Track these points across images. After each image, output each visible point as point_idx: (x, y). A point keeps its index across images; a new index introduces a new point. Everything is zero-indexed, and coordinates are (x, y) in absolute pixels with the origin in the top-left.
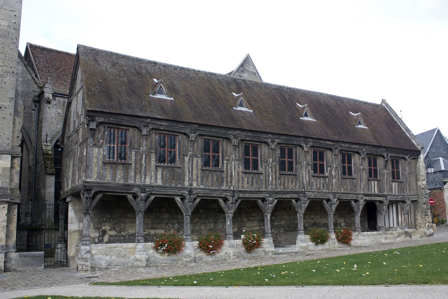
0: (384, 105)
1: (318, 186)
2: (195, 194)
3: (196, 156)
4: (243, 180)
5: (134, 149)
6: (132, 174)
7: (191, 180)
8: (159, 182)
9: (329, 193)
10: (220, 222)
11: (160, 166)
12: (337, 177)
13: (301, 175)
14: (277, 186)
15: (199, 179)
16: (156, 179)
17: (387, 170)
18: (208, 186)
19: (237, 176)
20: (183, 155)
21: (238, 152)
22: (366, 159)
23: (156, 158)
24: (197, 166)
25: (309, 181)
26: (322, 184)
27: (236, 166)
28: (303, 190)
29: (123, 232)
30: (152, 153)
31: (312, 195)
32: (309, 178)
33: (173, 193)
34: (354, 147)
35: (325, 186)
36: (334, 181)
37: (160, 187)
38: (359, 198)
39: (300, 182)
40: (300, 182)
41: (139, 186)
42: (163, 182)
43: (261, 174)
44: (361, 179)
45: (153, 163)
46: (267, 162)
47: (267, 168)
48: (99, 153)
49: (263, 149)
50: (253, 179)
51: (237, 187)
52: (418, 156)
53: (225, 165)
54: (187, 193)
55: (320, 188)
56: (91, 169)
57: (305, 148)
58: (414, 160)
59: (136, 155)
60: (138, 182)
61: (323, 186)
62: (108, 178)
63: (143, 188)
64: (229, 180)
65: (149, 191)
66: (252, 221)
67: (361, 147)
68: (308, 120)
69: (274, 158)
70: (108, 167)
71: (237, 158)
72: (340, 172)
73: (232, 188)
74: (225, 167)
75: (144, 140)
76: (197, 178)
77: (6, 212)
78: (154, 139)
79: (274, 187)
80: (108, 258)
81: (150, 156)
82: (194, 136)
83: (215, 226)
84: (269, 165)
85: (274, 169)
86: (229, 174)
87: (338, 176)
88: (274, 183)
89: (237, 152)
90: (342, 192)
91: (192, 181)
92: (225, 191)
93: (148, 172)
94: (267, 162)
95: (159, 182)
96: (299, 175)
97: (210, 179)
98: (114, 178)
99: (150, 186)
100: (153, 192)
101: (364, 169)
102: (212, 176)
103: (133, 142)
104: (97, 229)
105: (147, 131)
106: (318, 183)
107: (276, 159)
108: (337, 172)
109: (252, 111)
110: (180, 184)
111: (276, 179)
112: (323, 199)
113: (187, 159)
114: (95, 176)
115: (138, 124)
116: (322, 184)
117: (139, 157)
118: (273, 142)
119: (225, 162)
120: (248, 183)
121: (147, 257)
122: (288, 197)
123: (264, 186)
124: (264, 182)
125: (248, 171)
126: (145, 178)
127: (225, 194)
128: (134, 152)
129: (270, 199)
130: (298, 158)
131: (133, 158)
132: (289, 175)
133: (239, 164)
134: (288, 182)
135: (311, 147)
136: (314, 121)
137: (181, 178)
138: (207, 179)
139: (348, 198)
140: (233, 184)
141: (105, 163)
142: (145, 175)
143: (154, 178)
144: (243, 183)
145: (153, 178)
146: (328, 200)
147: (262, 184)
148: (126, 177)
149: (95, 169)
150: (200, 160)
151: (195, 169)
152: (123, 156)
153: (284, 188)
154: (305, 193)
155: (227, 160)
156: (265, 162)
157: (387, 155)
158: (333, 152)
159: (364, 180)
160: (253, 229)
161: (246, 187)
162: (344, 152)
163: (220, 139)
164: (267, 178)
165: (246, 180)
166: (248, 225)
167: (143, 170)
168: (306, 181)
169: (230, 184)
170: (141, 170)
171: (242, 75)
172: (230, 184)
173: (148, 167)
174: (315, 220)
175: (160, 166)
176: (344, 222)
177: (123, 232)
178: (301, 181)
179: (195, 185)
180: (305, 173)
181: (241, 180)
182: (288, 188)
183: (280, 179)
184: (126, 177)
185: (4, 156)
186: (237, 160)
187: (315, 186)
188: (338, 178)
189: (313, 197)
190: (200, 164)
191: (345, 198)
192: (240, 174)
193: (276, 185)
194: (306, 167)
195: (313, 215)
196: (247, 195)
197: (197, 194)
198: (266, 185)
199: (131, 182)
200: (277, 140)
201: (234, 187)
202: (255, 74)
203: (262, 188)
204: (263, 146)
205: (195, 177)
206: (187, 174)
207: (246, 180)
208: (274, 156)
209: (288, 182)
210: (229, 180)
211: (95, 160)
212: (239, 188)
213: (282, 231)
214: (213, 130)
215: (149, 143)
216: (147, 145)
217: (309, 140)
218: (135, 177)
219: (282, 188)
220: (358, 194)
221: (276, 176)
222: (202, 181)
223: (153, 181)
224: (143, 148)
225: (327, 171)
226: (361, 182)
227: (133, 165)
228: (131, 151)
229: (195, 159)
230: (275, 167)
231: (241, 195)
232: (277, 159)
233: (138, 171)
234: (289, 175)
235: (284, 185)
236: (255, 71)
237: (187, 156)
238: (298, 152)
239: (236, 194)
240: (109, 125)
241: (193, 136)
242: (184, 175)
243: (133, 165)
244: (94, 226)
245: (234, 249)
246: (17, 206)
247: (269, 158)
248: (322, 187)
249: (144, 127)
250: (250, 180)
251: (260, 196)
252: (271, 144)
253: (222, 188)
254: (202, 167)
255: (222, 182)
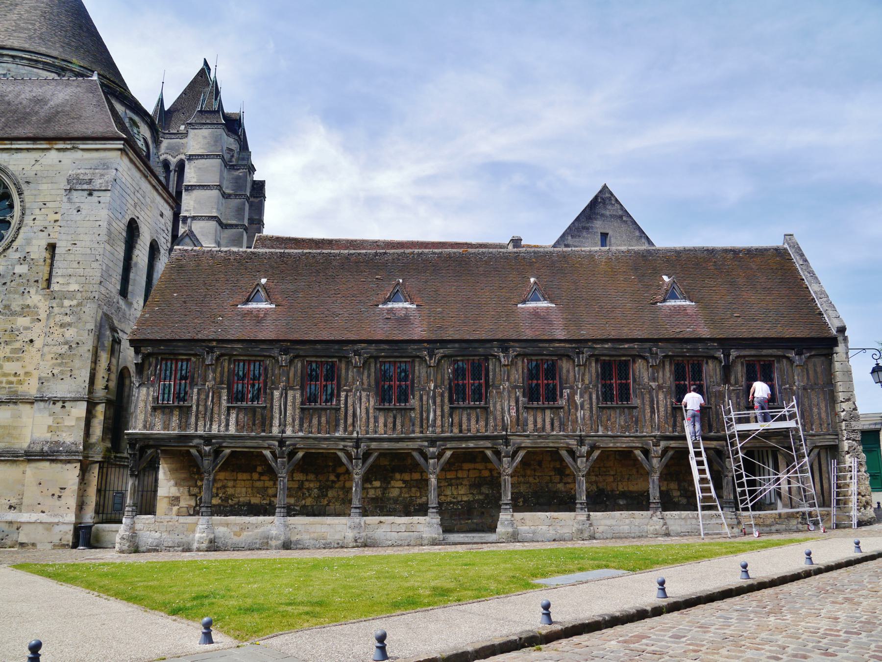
0: (786, 246)
1: (539, 425)
2: (289, 445)
3: (292, 388)
4: (376, 420)
5: (197, 384)
6: (193, 420)
7: (283, 425)
8: (232, 430)
9: (567, 436)
10: (393, 487)
11: (234, 408)
12: (587, 406)
13: (499, 407)
14: (446, 429)
15: (297, 422)
16: (227, 425)
17: (732, 386)
18: (311, 433)
19: (364, 415)
20: (271, 389)
21: (369, 376)
22: (667, 367)
23: (228, 396)
24: (294, 403)
25: (518, 416)
26: (548, 420)
27: (364, 400)
28: (504, 433)
29: (230, 501)
30: (223, 388)
31: (527, 443)
32: (518, 411)
33: (255, 445)
34: (626, 346)
35: (556, 424)
36: (580, 414)
37: (233, 437)
38: (647, 444)
39: (495, 419)
40: (495, 419)
41: (201, 437)
42: (237, 430)
43: (413, 409)
44: (652, 408)
45: (224, 404)
46: (424, 389)
47: (425, 398)
48: (148, 394)
49: (417, 368)
50: (395, 418)
51: (364, 433)
52: (832, 349)
53: (343, 399)
54: (277, 443)
55: (543, 428)
56: (136, 417)
57: (503, 360)
58: (823, 358)
59: (198, 394)
60: (200, 432)
61: (552, 424)
62: (158, 430)
63: (208, 440)
64: (350, 421)
65: (217, 443)
66: (457, 485)
67: (647, 345)
68: (543, 308)
69: (439, 381)
70: (159, 411)
71: (365, 386)
72: (594, 396)
73: (355, 435)
74: (342, 402)
75: (210, 371)
76: (294, 421)
77: (77, 472)
78: (226, 370)
79: (439, 430)
80: (157, 535)
81: (220, 393)
82: (286, 360)
83: (383, 494)
84: (428, 395)
85: (438, 400)
86: (350, 412)
87: (591, 404)
88: (439, 422)
89: (365, 378)
90: (600, 433)
91: (285, 426)
92: (343, 439)
93: (216, 416)
94: (424, 389)
95: (232, 430)
96: (495, 407)
97: (315, 421)
98: (166, 427)
99: (215, 437)
100: (224, 444)
101: (660, 387)
102: (320, 417)
103: (196, 375)
104: (193, 495)
105: (212, 359)
106: (539, 420)
107: (443, 382)
108: (586, 397)
109: (415, 306)
110: (264, 431)
111: (443, 416)
112: (558, 448)
113: (277, 394)
114: (141, 425)
115: (198, 350)
116: (548, 420)
117: (203, 397)
118: (431, 355)
119: (343, 394)
120: (385, 425)
121: (212, 536)
122: (471, 445)
123: (417, 429)
124: (417, 422)
125: (387, 406)
126: (211, 425)
127: (343, 443)
128: (195, 390)
129: (431, 449)
130: (491, 377)
131: (195, 397)
132: (471, 408)
133: (368, 396)
134: (469, 420)
135: (516, 356)
136: (548, 308)
137: (266, 423)
138: (310, 422)
139: (618, 445)
140: (358, 429)
141: (154, 409)
142: (211, 421)
143: (226, 425)
144: (375, 426)
145: (223, 425)
146: (572, 453)
147: (413, 425)
148: (184, 425)
149: (141, 417)
150: (298, 395)
151: (289, 408)
152: (182, 396)
153: (461, 431)
154: (507, 439)
155: (347, 391)
156: (420, 390)
157: (727, 356)
158: (574, 361)
159: (662, 409)
160: (459, 499)
161: (381, 433)
162: (607, 358)
163: (335, 360)
164: (425, 415)
165: (381, 421)
166: (448, 493)
167: (208, 414)
168: (511, 417)
169: (351, 429)
170: (205, 414)
171: (587, 225)
172: (351, 429)
173: (216, 409)
174: (601, 486)
175: (234, 408)
176: (679, 490)
177: (230, 501)
178: (499, 417)
179: (289, 432)
180: (506, 405)
181: (372, 420)
182: (469, 430)
183: (451, 415)
184: (184, 425)
185: (79, 403)
186: (364, 390)
187: (531, 426)
188: (591, 408)
189: (529, 445)
190: (298, 400)
191: (611, 445)
192: (371, 411)
193: (442, 426)
194: (509, 392)
195: (596, 476)
196: (386, 445)
197: (294, 445)
198: (422, 426)
199: (191, 431)
200: (442, 351)
201: (358, 433)
202: (621, 217)
203: (413, 432)
204: (417, 364)
205: (289, 420)
206: (277, 415)
207: (381, 421)
208: (439, 377)
209: (469, 420)
210: (350, 421)
211: (141, 405)
212: (367, 433)
213: (521, 504)
214: (319, 346)
215: (218, 375)
216: (214, 379)
217: (512, 344)
218: (196, 424)
219: (456, 430)
220: (645, 436)
221: (442, 411)
222: (301, 425)
223: (222, 429)
224: (208, 384)
225: (561, 396)
226: (653, 412)
227: (194, 407)
228: (191, 388)
229: (290, 393)
230: (442, 395)
231: (374, 445)
232: (446, 382)
233: (200, 416)
234: (471, 408)
235: (460, 426)
236: (620, 213)
237: (277, 389)
238: (491, 367)
239: (362, 445)
240: (163, 356)
241: (283, 359)
242: (272, 418)
243: (194, 407)
244: (189, 491)
245: (356, 531)
246: (98, 465)
247: (428, 380)
248: (548, 426)
249: (208, 353)
250: (390, 420)
251: (411, 445)
252: (427, 358)
253: (337, 435)
254: (302, 403)
255: (337, 425)
